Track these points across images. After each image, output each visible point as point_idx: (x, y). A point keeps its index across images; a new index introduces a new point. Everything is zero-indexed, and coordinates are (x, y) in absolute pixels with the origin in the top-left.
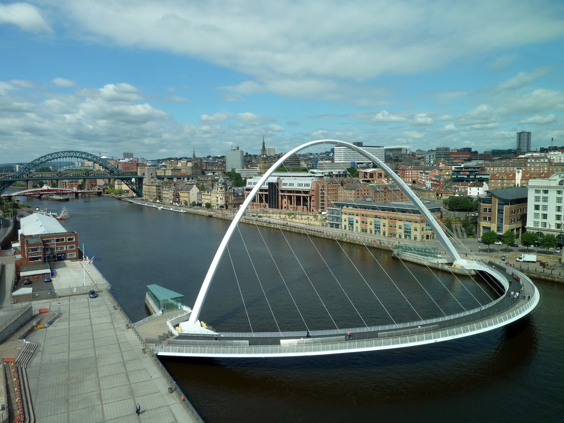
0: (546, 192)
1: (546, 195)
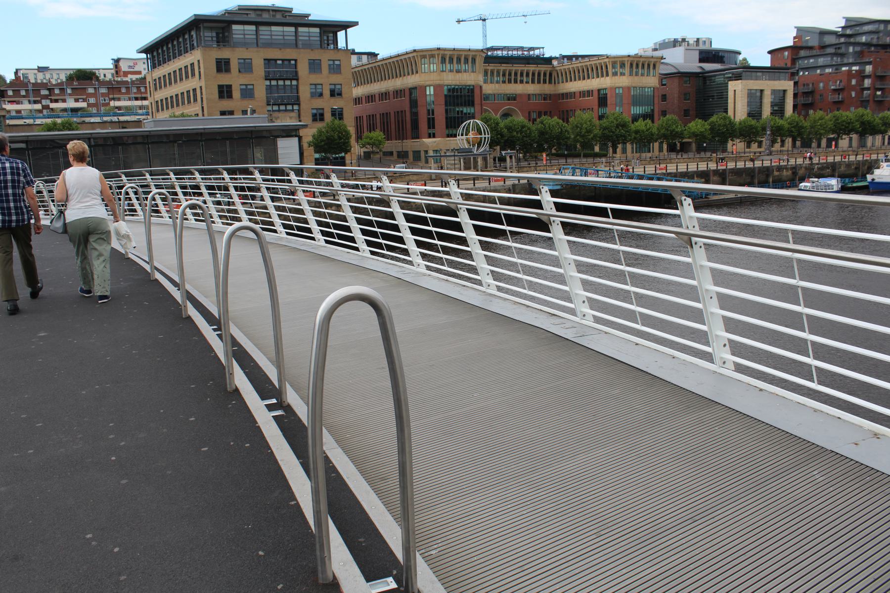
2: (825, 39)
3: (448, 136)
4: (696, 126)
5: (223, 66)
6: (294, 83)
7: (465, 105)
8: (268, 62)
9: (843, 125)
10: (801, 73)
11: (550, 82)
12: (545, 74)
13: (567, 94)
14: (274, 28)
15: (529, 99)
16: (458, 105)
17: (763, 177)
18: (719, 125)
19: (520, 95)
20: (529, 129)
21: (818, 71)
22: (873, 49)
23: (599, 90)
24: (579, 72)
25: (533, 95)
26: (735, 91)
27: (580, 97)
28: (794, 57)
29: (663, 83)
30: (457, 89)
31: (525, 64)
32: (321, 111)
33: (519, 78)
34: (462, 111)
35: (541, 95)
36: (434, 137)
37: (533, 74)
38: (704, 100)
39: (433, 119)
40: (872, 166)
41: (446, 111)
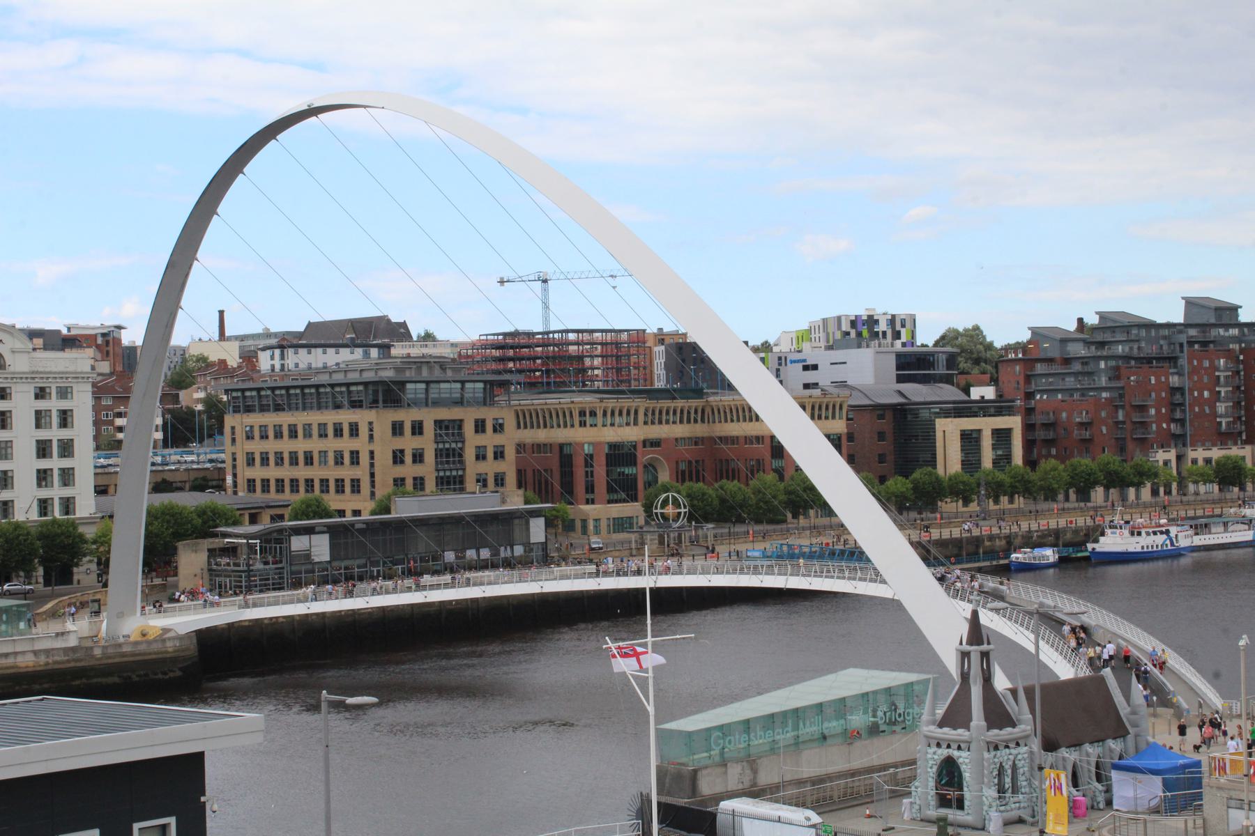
2: (1068, 348)
3: (609, 502)
4: (896, 484)
5: (397, 429)
6: (460, 445)
7: (627, 466)
8: (439, 424)
9: (1082, 477)
10: (1038, 397)
14: (443, 386)
17: (971, 549)
18: (924, 483)
19: (666, 440)
20: (710, 496)
21: (1060, 396)
22: (1133, 363)
25: (681, 439)
26: (944, 431)
27: (746, 444)
28: (1029, 373)
29: (850, 416)
30: (619, 446)
33: (664, 418)
34: (623, 472)
36: (593, 502)
38: (905, 440)
40: (1095, 533)
41: (607, 471)
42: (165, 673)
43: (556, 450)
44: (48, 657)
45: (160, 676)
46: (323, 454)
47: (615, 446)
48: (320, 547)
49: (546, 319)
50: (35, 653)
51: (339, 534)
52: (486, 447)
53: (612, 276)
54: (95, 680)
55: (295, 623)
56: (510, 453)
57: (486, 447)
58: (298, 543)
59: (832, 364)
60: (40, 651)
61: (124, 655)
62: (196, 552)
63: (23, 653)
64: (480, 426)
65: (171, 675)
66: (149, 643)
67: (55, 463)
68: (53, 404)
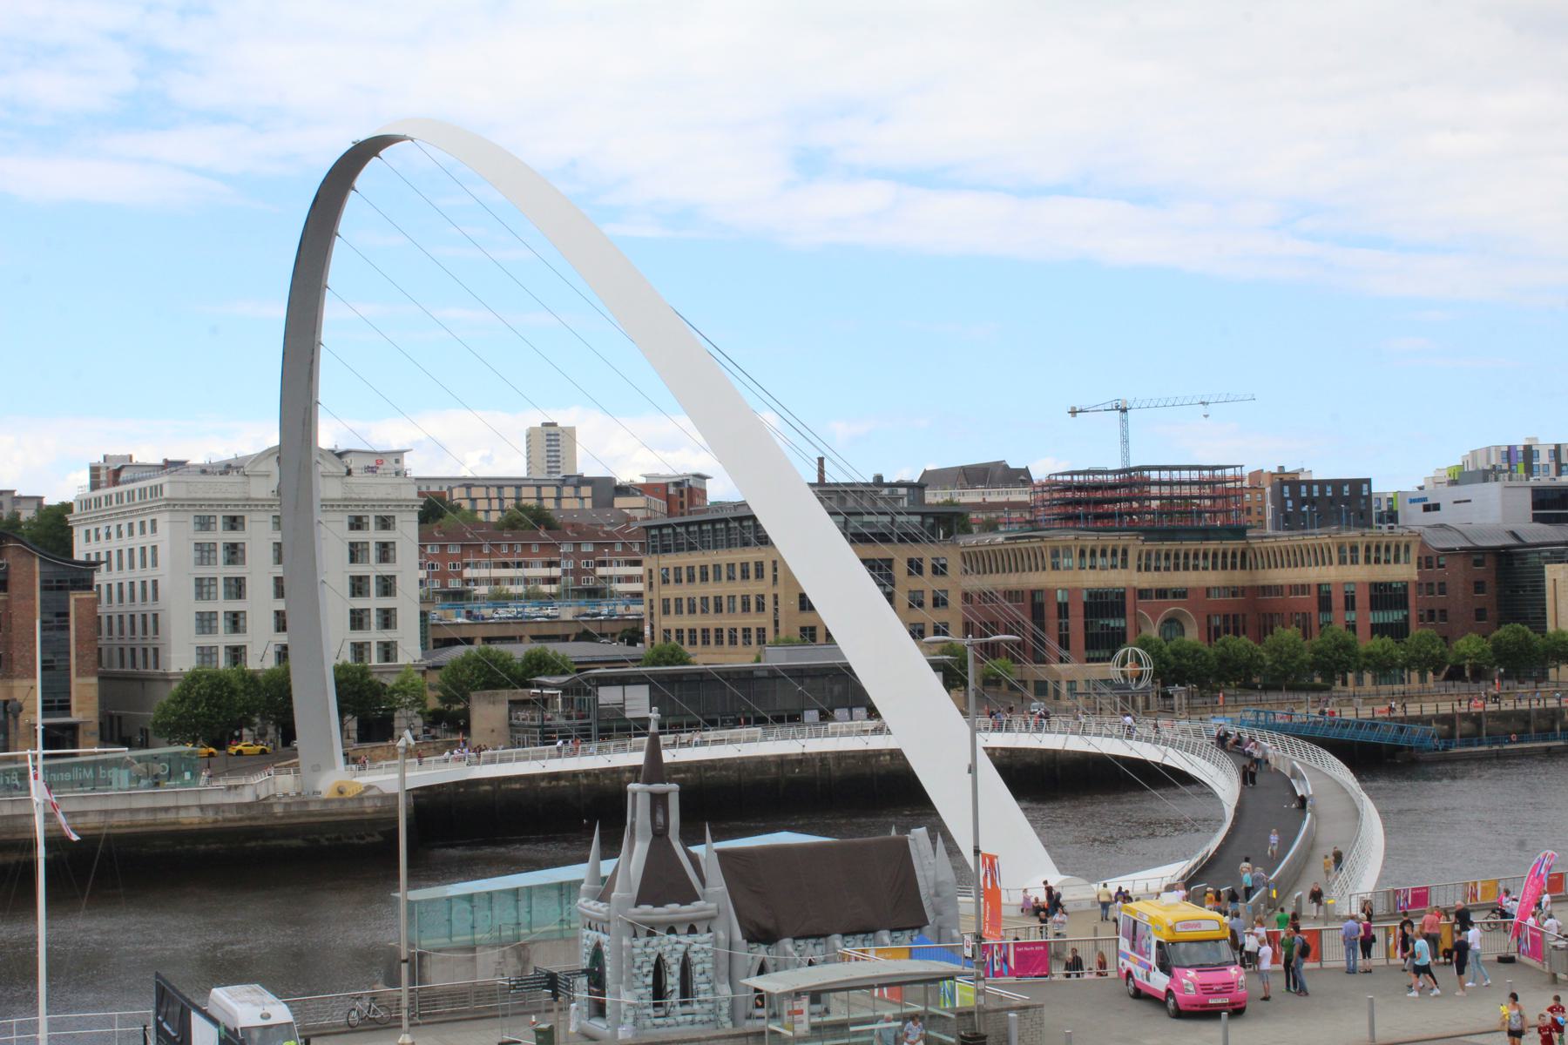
0: (234, 523)
1: (233, 537)
3: (1089, 660)
4: (1469, 644)
7: (1113, 617)
11: (1243, 567)
12: (1234, 555)
13: (1270, 587)
15: (1208, 595)
16: (1102, 617)
17: (1544, 724)
18: (1508, 642)
19: (1194, 589)
20: (1205, 654)
23: (1319, 586)
24: (1288, 555)
25: (1215, 588)
27: (1291, 594)
29: (1441, 563)
30: (1101, 594)
31: (1202, 540)
32: (920, 627)
33: (1191, 562)
35: (1228, 588)
37: (1215, 555)
38: (1512, 591)
39: (1067, 636)
41: (1086, 624)
42: (362, 838)
43: (1028, 598)
44: (217, 813)
45: (356, 841)
46: (731, 599)
47: (1096, 593)
48: (638, 702)
49: (1126, 454)
50: (202, 808)
51: (662, 690)
52: (922, 592)
53: (1203, 403)
54: (274, 842)
55: (581, 788)
56: (955, 600)
57: (922, 592)
58: (608, 695)
59: (1455, 502)
60: (208, 806)
61: (310, 814)
62: (494, 703)
63: (187, 807)
64: (915, 567)
65: (369, 839)
66: (344, 801)
67: (373, 602)
68: (372, 536)
